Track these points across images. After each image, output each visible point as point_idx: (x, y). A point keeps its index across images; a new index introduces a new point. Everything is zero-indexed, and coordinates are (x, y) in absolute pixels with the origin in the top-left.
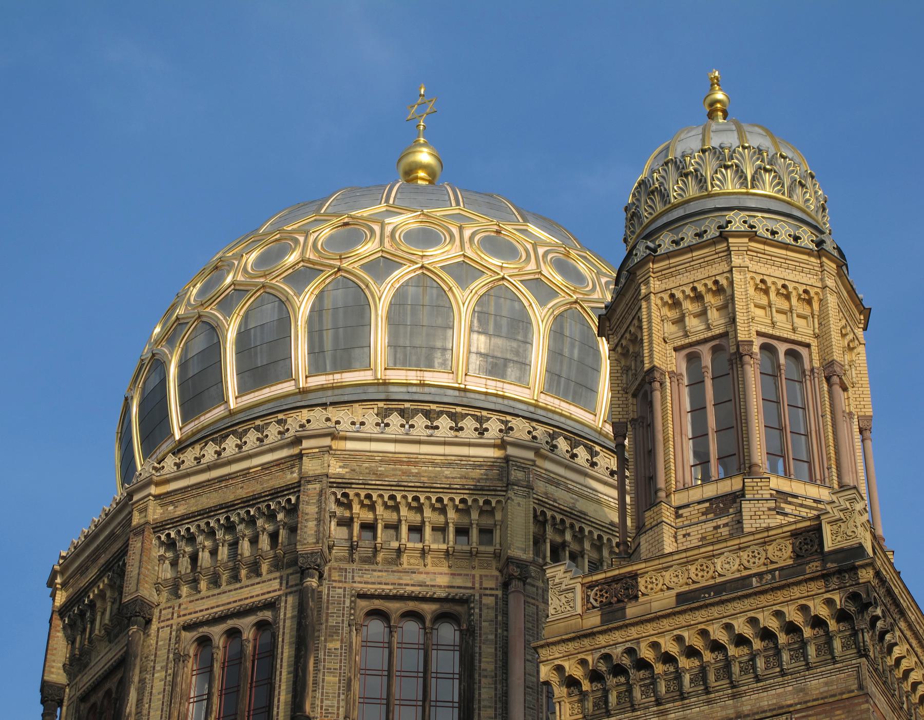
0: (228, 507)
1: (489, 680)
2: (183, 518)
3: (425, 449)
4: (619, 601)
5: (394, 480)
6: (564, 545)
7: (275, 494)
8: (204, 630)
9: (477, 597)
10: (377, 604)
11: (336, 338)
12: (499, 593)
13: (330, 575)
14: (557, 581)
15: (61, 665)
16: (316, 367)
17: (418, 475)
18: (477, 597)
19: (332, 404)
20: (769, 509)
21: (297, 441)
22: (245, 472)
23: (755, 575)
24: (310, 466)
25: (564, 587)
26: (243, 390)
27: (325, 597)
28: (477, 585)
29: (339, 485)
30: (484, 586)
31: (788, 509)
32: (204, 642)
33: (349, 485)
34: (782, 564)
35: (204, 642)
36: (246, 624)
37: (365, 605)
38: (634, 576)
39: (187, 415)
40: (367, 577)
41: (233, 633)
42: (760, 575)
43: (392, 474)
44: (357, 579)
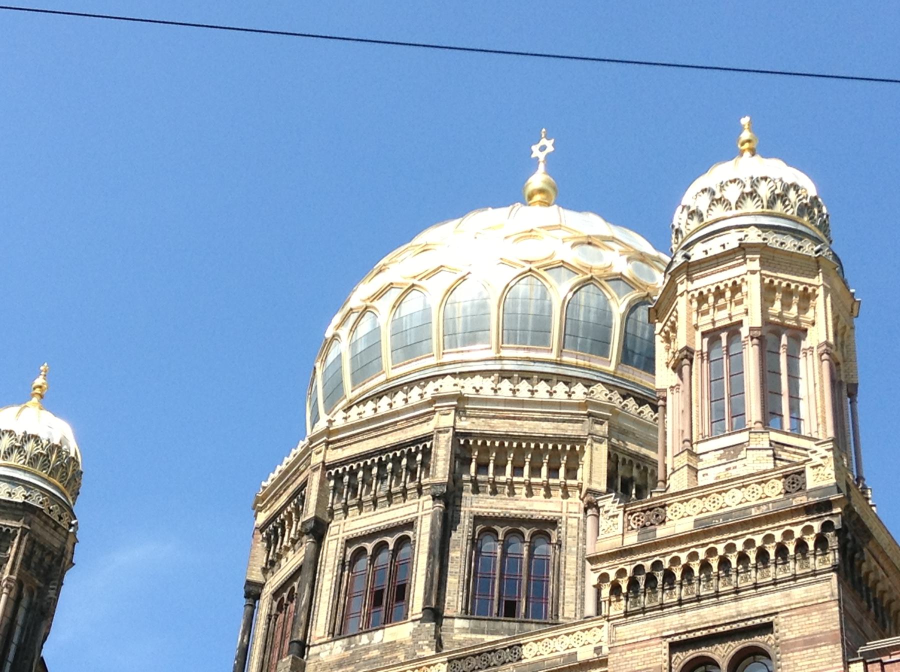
1: (572, 582)
4: (652, 524)
6: (632, 480)
7: (416, 441)
9: (564, 519)
11: (465, 323)
12: (581, 516)
13: (454, 502)
14: (606, 509)
15: (259, 569)
18: (564, 519)
19: (460, 373)
20: (768, 456)
23: (753, 506)
25: (611, 513)
27: (450, 518)
28: (564, 511)
30: (570, 510)
31: (784, 456)
34: (774, 498)
39: (355, 383)
42: (758, 506)
43: (502, 426)
44: (474, 504)
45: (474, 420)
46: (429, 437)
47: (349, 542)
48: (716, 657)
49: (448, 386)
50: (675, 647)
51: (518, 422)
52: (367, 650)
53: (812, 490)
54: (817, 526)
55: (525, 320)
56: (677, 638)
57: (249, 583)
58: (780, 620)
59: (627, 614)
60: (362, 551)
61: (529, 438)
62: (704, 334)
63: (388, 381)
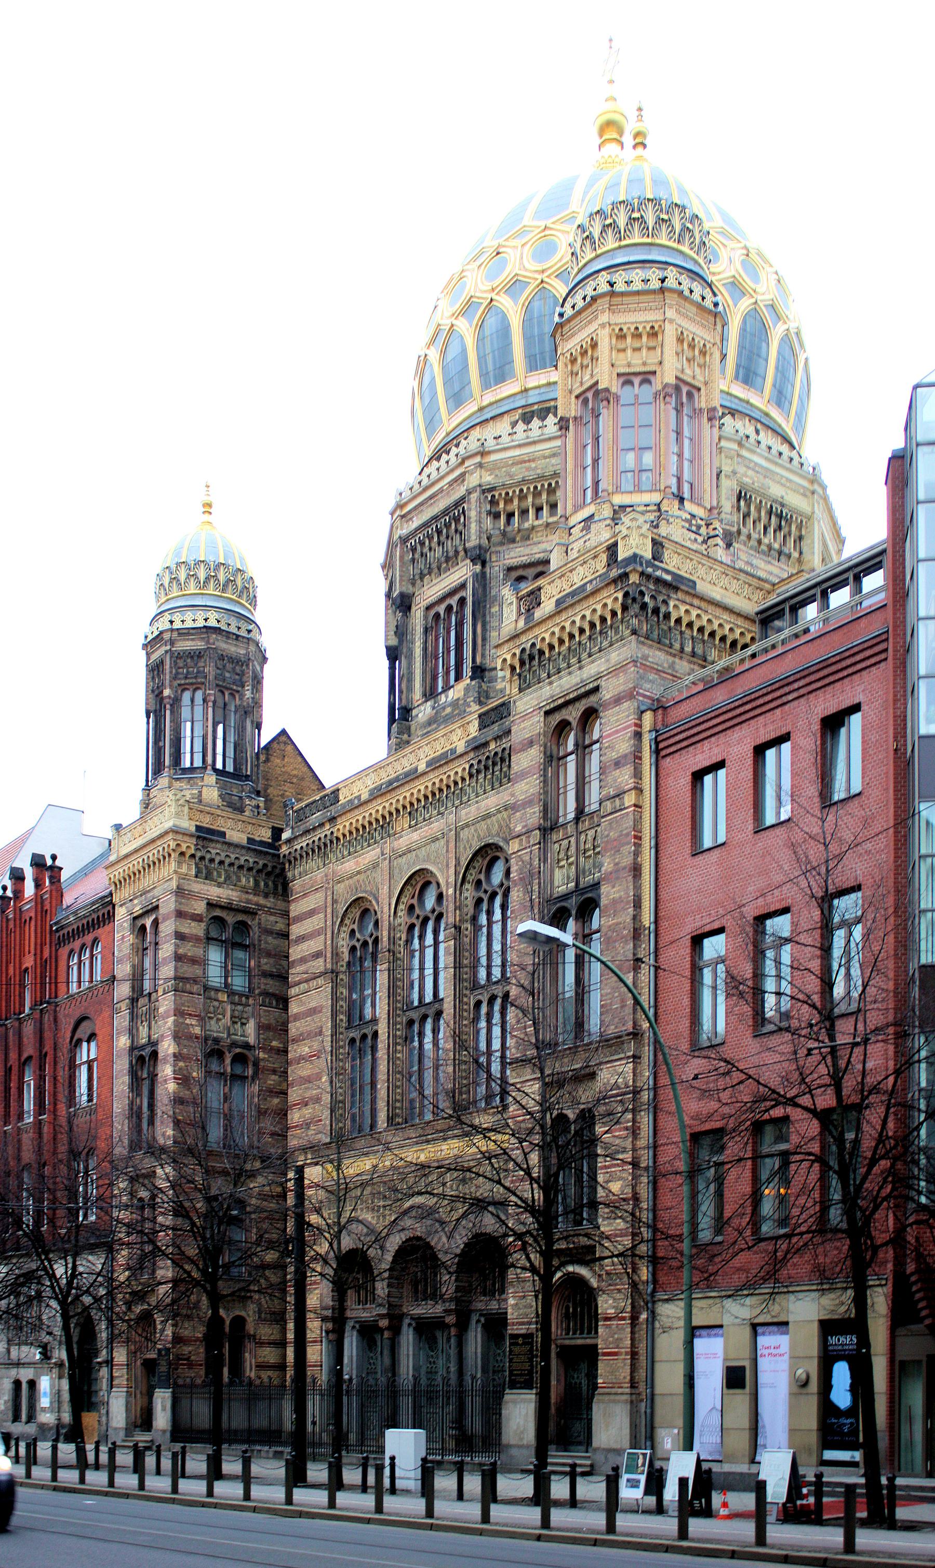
0: (435, 518)
2: (417, 530)
3: (539, 447)
5: (519, 477)
17: (536, 468)
19: (492, 418)
22: (441, 490)
33: (493, 489)
43: (519, 473)
45: (497, 472)
46: (462, 499)
47: (428, 608)
48: (571, 719)
49: (471, 444)
50: (547, 713)
51: (533, 465)
53: (623, 561)
54: (620, 595)
55: (541, 341)
56: (548, 708)
58: (603, 683)
60: (437, 615)
61: (541, 478)
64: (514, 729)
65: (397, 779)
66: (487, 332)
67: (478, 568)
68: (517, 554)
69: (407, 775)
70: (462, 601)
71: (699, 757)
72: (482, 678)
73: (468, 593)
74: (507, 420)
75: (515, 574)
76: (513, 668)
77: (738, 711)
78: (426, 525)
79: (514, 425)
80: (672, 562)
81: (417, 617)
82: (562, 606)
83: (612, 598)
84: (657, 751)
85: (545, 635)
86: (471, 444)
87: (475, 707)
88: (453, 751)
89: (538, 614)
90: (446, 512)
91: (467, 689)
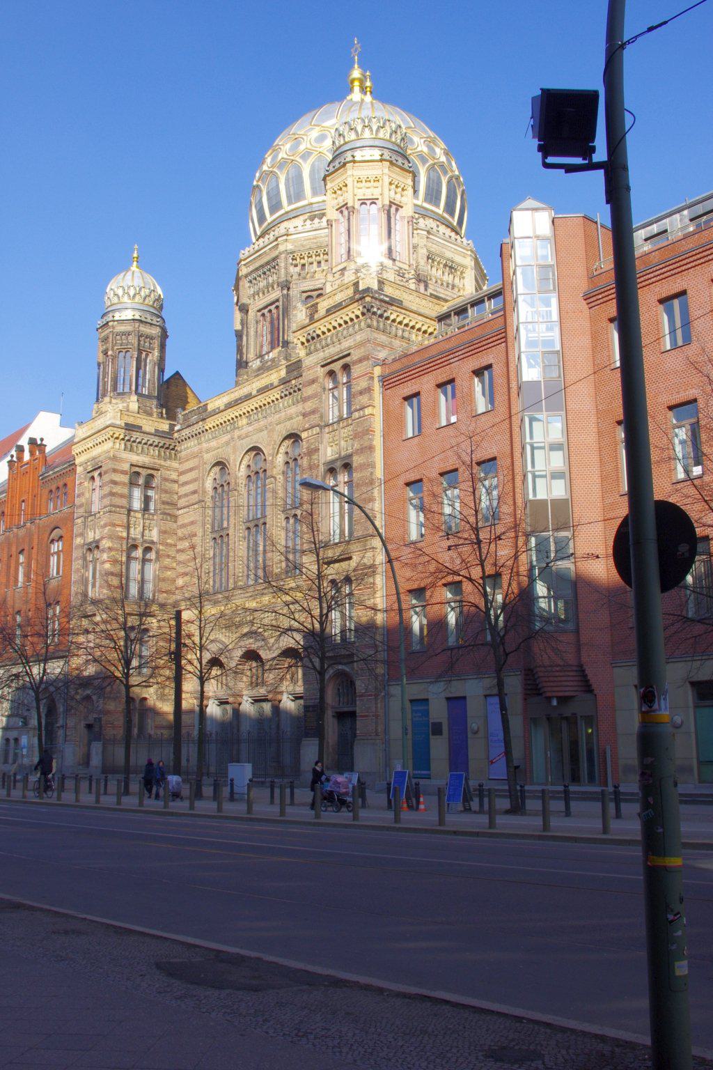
0: (262, 266)
2: (252, 272)
5: (308, 247)
8: (269, 308)
10: (309, 294)
16: (290, 202)
17: (317, 243)
21: (276, 239)
24: (281, 248)
26: (271, 214)
29: (291, 253)
32: (263, 315)
35: (263, 315)
36: (272, 307)
37: (305, 295)
38: (317, 304)
40: (304, 285)
41: (270, 311)
47: (259, 311)
51: (315, 241)
52: (267, 362)
57: (236, 331)
58: (352, 351)
59: (308, 355)
62: (337, 210)
63: (269, 224)
64: (304, 374)
65: (240, 399)
66: (290, 176)
67: (285, 292)
68: (308, 285)
69: (246, 396)
70: (277, 307)
71: (406, 390)
72: (287, 347)
73: (280, 304)
74: (302, 218)
75: (305, 295)
76: (303, 343)
77: (426, 367)
78: (257, 269)
79: (305, 221)
80: (389, 291)
81: (251, 314)
82: (330, 312)
83: (357, 309)
84: (383, 386)
85: (320, 327)
86: (281, 229)
87: (283, 362)
88: (272, 384)
89: (316, 317)
90: (268, 263)
91: (280, 352)
